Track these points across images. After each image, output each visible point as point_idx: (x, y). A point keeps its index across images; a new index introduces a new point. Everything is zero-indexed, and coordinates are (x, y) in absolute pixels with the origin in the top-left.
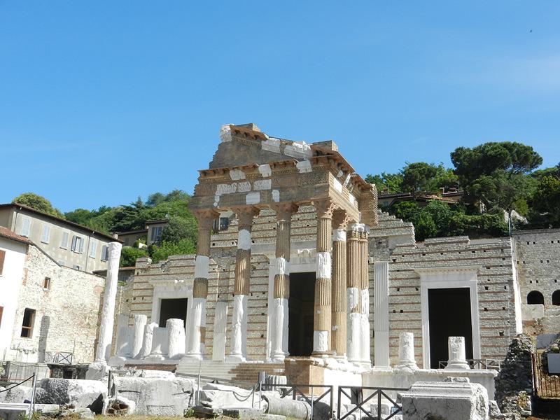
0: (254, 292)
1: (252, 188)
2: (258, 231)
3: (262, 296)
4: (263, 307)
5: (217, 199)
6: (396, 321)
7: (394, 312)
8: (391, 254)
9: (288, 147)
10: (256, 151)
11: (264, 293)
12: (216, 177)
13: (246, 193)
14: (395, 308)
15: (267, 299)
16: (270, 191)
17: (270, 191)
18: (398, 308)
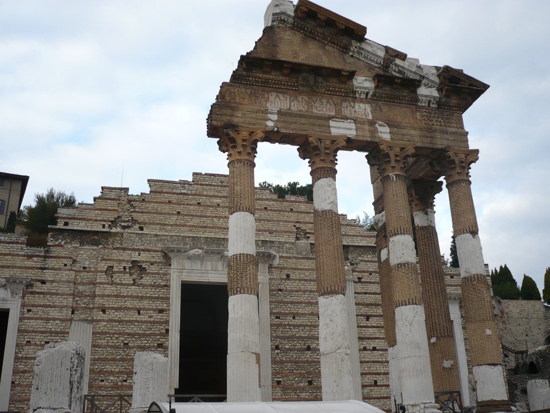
0: (144, 309)
1: (339, 111)
2: (148, 212)
3: (158, 317)
4: (161, 334)
5: (275, 117)
6: (367, 362)
7: (365, 349)
8: (354, 271)
9: (398, 61)
10: (337, 54)
11: (161, 311)
12: (274, 77)
13: (330, 118)
14: (365, 343)
15: (167, 322)
16: (372, 123)
17: (372, 123)
18: (370, 345)
